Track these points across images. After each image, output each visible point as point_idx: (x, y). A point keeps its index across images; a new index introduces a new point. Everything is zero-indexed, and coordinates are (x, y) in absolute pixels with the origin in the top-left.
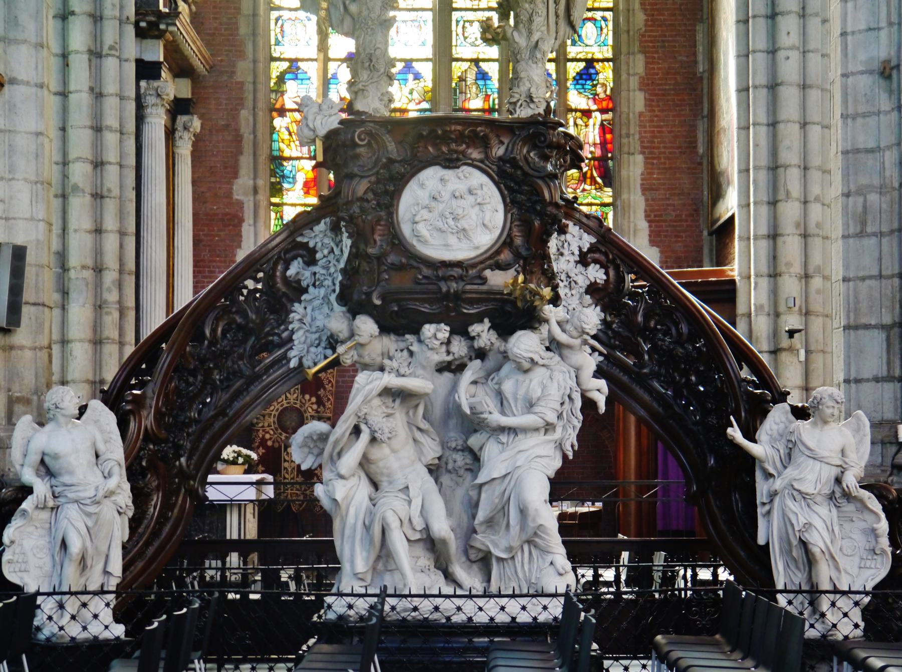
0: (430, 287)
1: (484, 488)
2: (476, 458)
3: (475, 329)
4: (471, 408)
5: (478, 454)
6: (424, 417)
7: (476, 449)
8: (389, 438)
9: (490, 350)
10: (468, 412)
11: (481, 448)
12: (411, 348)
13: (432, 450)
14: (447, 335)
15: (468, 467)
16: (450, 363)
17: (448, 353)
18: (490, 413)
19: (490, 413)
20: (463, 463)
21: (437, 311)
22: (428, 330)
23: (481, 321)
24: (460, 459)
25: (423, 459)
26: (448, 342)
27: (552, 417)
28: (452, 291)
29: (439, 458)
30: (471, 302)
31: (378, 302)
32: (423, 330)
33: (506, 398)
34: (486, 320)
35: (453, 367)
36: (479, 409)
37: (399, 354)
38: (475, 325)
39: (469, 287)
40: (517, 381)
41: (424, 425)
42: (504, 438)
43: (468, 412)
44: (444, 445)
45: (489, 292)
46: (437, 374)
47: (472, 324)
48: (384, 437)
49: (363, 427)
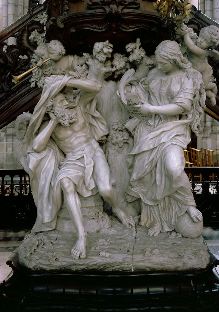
0: (98, 11)
1: (138, 158)
2: (131, 136)
3: (129, 47)
4: (128, 101)
5: (133, 133)
6: (97, 109)
7: (131, 130)
8: (70, 124)
9: (140, 64)
10: (126, 103)
11: (134, 129)
12: (87, 62)
13: (101, 130)
14: (111, 50)
15: (125, 141)
16: (113, 73)
17: (112, 66)
18: (142, 104)
19: (142, 104)
20: (122, 139)
21: (104, 30)
22: (98, 46)
23: (134, 41)
24: (121, 137)
25: (96, 137)
26: (111, 59)
27: (187, 104)
28: (114, 12)
29: (107, 136)
30: (129, 23)
31: (62, 26)
32: (95, 47)
33: (153, 94)
34: (138, 40)
35: (116, 77)
36: (134, 101)
37: (79, 68)
38: (131, 43)
39: (126, 10)
40: (161, 80)
41: (97, 114)
42: (151, 122)
43: (126, 103)
44: (108, 127)
45: (141, 15)
46: (105, 82)
47: (128, 43)
48: (66, 123)
49: (51, 115)
